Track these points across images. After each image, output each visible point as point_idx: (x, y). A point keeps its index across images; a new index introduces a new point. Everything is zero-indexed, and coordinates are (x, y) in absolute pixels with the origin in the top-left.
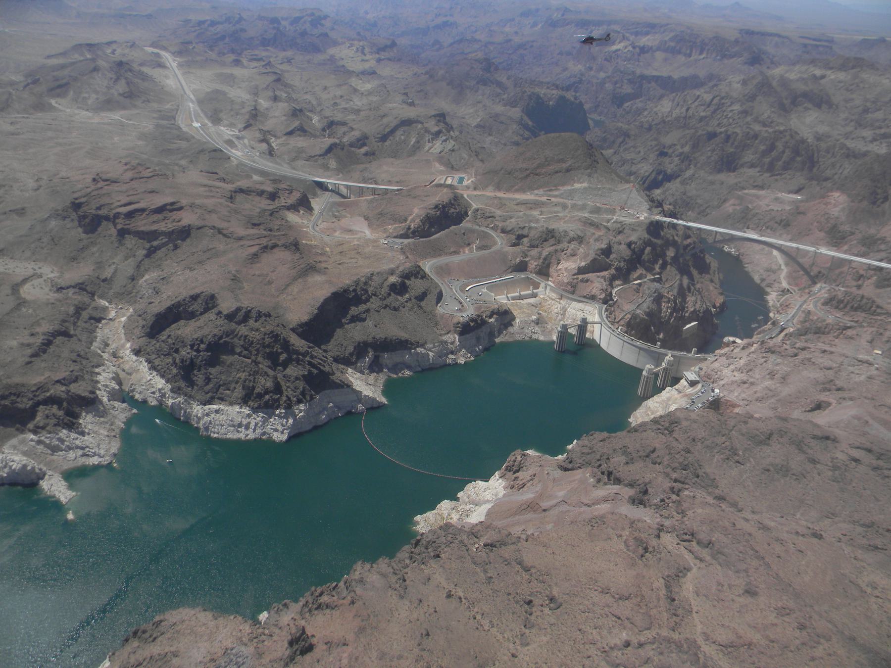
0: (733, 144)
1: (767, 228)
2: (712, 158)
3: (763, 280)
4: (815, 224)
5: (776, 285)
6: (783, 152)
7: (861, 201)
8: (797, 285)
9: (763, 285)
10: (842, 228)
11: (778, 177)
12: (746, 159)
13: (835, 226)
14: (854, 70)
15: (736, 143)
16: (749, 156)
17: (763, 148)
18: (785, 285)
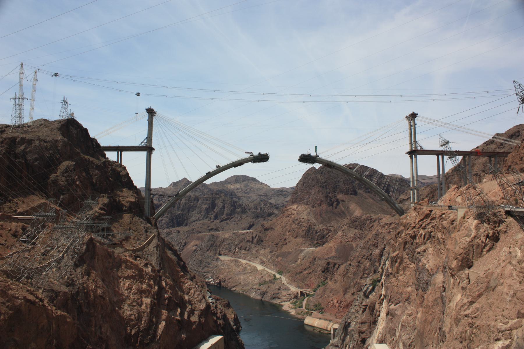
0: (179, 208)
1: (240, 249)
2: (164, 221)
3: (263, 294)
4: (287, 233)
5: (284, 293)
6: (224, 207)
7: (320, 205)
8: (308, 286)
9: (267, 298)
10: (317, 228)
11: (228, 221)
12: (193, 218)
13: (309, 229)
14: (245, 183)
15: (181, 206)
16: (195, 215)
17: (205, 206)
18: (294, 289)
